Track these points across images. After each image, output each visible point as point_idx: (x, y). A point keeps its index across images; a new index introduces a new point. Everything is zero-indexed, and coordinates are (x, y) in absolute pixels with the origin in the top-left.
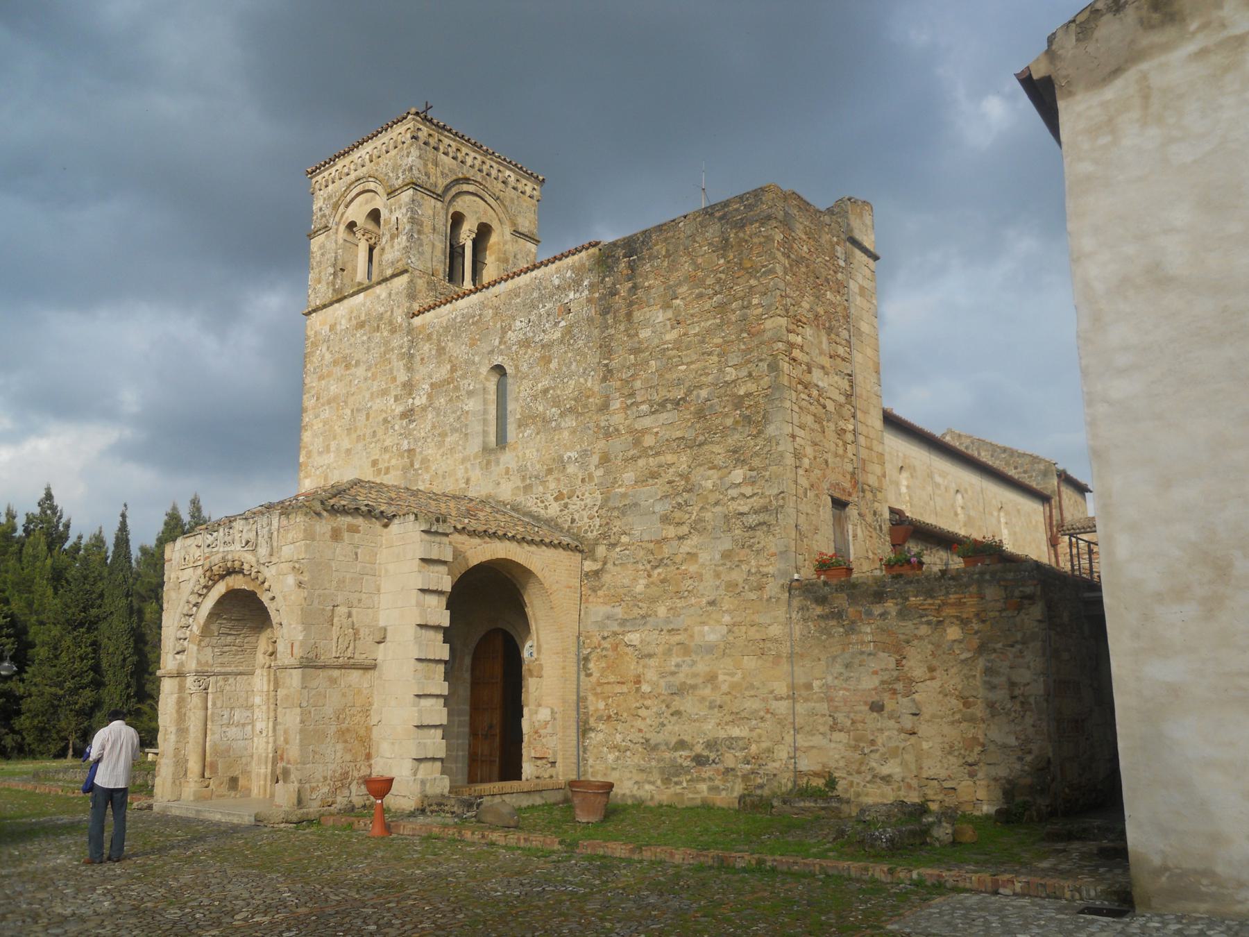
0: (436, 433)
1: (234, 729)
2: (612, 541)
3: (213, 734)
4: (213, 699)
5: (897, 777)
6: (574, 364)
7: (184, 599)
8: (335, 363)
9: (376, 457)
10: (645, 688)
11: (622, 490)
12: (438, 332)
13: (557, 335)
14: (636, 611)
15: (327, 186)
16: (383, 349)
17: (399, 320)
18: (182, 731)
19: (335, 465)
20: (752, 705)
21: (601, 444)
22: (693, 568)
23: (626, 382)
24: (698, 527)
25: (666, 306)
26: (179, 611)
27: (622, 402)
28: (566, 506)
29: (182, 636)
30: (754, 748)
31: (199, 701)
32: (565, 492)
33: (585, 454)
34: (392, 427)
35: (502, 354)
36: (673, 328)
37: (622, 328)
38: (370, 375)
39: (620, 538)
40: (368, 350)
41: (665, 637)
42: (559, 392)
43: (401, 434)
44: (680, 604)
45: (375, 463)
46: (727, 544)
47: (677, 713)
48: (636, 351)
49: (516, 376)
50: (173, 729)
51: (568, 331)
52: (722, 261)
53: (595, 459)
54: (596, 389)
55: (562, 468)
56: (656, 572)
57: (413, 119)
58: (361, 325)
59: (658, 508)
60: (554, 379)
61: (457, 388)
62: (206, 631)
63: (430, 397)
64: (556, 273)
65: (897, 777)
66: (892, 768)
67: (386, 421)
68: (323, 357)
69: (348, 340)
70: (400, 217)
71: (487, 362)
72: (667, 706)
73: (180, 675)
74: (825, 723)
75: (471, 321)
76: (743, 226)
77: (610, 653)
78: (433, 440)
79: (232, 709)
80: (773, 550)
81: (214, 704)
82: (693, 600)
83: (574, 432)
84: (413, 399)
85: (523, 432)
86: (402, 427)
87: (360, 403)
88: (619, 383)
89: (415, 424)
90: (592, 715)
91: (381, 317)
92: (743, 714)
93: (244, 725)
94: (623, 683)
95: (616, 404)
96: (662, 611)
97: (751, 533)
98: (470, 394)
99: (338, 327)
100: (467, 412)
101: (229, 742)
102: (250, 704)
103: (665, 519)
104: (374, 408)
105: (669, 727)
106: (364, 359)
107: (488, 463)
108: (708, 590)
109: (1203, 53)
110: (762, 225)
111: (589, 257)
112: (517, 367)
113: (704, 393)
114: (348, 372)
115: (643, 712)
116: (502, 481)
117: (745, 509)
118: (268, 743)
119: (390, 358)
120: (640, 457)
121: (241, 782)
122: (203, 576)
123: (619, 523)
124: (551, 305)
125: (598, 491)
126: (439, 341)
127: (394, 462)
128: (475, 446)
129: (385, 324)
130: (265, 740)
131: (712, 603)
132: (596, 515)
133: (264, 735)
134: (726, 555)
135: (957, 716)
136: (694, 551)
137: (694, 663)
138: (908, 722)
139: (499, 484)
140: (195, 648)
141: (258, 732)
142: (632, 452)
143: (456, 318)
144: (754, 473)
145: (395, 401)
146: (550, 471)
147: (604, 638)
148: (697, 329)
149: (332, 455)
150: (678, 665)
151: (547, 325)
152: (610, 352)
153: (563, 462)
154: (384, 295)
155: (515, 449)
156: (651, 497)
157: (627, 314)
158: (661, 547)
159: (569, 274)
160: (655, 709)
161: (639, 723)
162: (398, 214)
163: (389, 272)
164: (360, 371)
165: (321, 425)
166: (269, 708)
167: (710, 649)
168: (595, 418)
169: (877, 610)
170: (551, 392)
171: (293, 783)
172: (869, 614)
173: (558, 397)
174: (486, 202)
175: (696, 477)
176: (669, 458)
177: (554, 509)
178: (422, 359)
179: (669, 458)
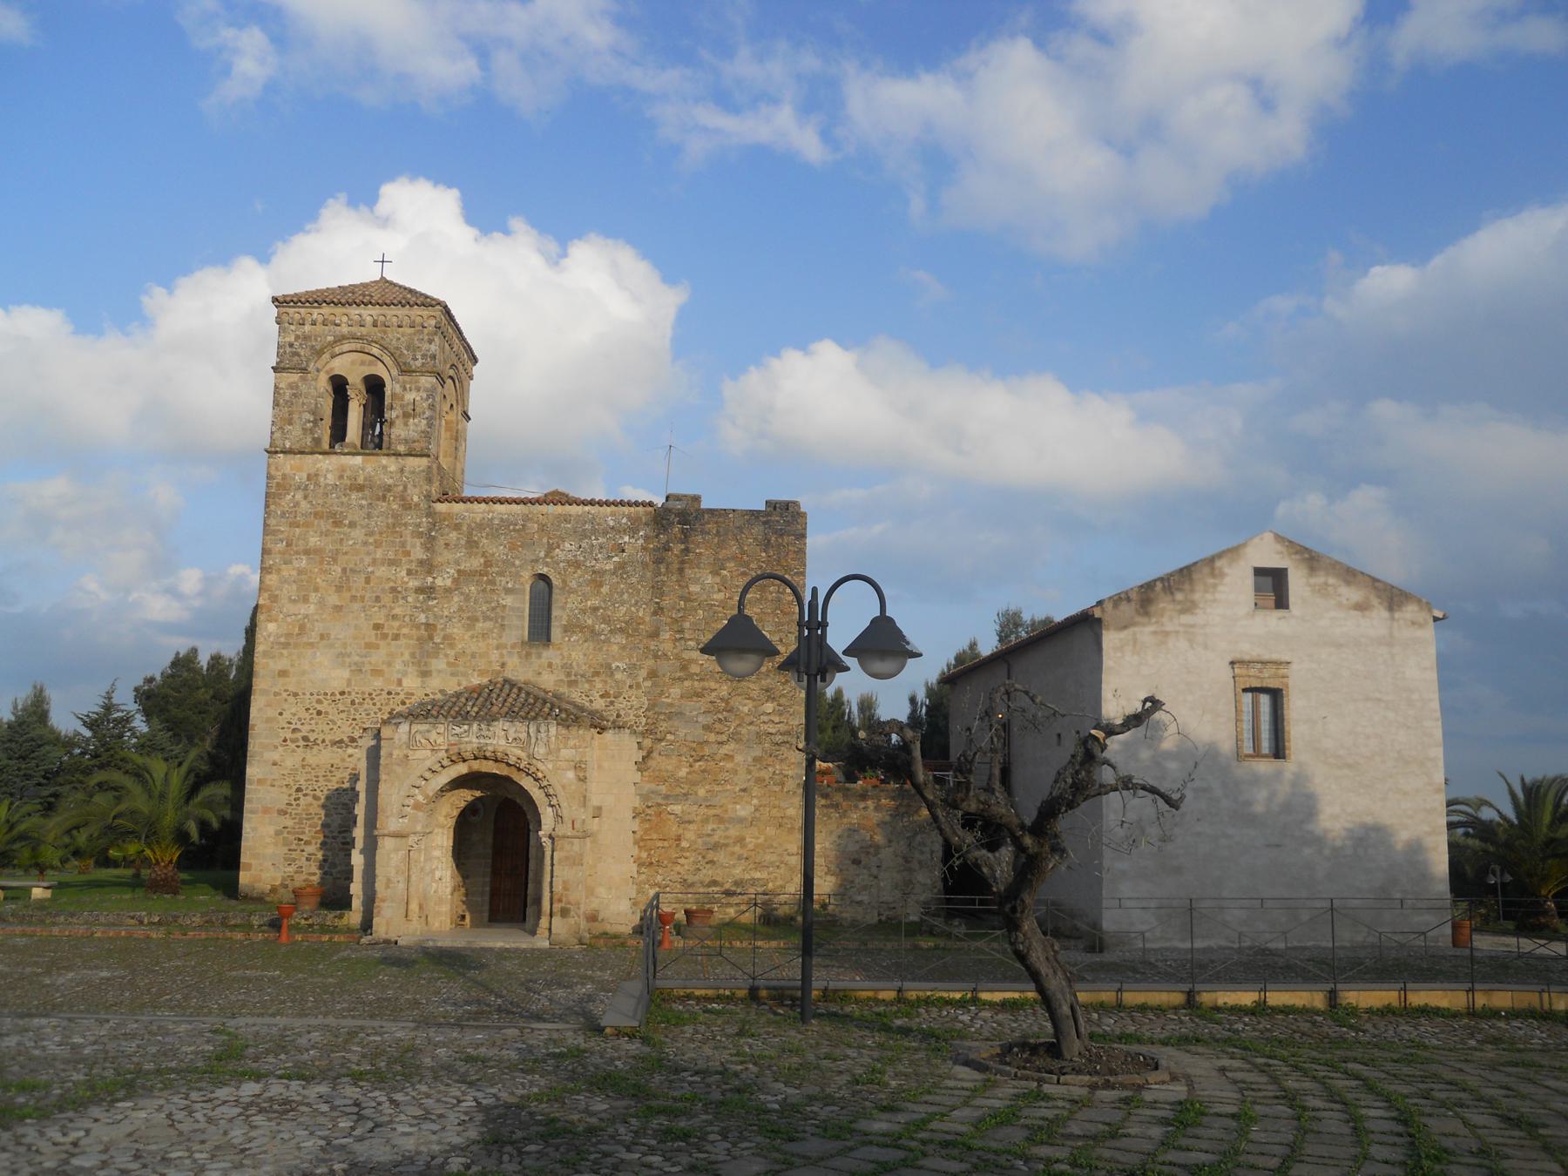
2: (659, 736)
5: (866, 902)
8: (316, 514)
9: (381, 622)
10: (684, 844)
11: (669, 701)
12: (469, 525)
13: (610, 567)
14: (678, 790)
16: (390, 521)
17: (416, 499)
19: (316, 617)
20: (769, 858)
21: (650, 662)
22: (729, 765)
24: (735, 737)
25: (715, 573)
28: (612, 703)
30: (770, 885)
32: (612, 692)
34: (405, 598)
36: (720, 591)
37: (674, 578)
40: (369, 516)
41: (703, 810)
42: (609, 613)
43: (416, 607)
44: (717, 788)
45: (377, 627)
46: (758, 753)
47: (712, 862)
48: (687, 600)
49: (563, 588)
51: (621, 566)
52: (764, 554)
53: (643, 673)
54: (647, 619)
56: (698, 764)
57: (441, 311)
58: (360, 488)
59: (700, 719)
60: (604, 601)
61: (492, 582)
63: (455, 581)
64: (611, 515)
65: (866, 902)
66: (864, 897)
67: (393, 590)
68: (297, 504)
72: (704, 857)
74: (822, 871)
75: (511, 527)
76: (782, 535)
77: (653, 818)
78: (460, 621)
80: (793, 760)
82: (729, 787)
83: (623, 648)
85: (570, 637)
87: (356, 564)
88: (669, 620)
89: (435, 602)
91: (388, 489)
92: (765, 864)
96: (702, 792)
97: (777, 747)
98: (508, 591)
100: (504, 606)
103: (707, 728)
104: (378, 574)
105: (704, 871)
107: (528, 655)
108: (741, 779)
109: (1155, 633)
110: (797, 539)
111: (647, 514)
112: (564, 582)
115: (682, 861)
116: (544, 672)
117: (773, 731)
124: (605, 540)
126: (470, 534)
127: (405, 631)
131: (744, 790)
134: (756, 759)
135: (902, 868)
136: (731, 753)
137: (727, 829)
138: (875, 871)
139: (540, 673)
141: (437, 878)
142: (678, 674)
143: (492, 519)
144: (781, 708)
145: (408, 574)
146: (597, 674)
147: (649, 807)
149: (312, 606)
150: (713, 830)
152: (662, 594)
153: (611, 668)
154: (393, 468)
155: (559, 649)
156: (695, 710)
157: (679, 569)
158: (703, 748)
159: (624, 520)
160: (692, 859)
161: (678, 868)
164: (358, 534)
165: (294, 573)
167: (741, 820)
168: (645, 641)
169: (862, 805)
172: (856, 807)
175: (736, 702)
176: (713, 685)
177: (599, 704)
178: (447, 545)
179: (713, 685)
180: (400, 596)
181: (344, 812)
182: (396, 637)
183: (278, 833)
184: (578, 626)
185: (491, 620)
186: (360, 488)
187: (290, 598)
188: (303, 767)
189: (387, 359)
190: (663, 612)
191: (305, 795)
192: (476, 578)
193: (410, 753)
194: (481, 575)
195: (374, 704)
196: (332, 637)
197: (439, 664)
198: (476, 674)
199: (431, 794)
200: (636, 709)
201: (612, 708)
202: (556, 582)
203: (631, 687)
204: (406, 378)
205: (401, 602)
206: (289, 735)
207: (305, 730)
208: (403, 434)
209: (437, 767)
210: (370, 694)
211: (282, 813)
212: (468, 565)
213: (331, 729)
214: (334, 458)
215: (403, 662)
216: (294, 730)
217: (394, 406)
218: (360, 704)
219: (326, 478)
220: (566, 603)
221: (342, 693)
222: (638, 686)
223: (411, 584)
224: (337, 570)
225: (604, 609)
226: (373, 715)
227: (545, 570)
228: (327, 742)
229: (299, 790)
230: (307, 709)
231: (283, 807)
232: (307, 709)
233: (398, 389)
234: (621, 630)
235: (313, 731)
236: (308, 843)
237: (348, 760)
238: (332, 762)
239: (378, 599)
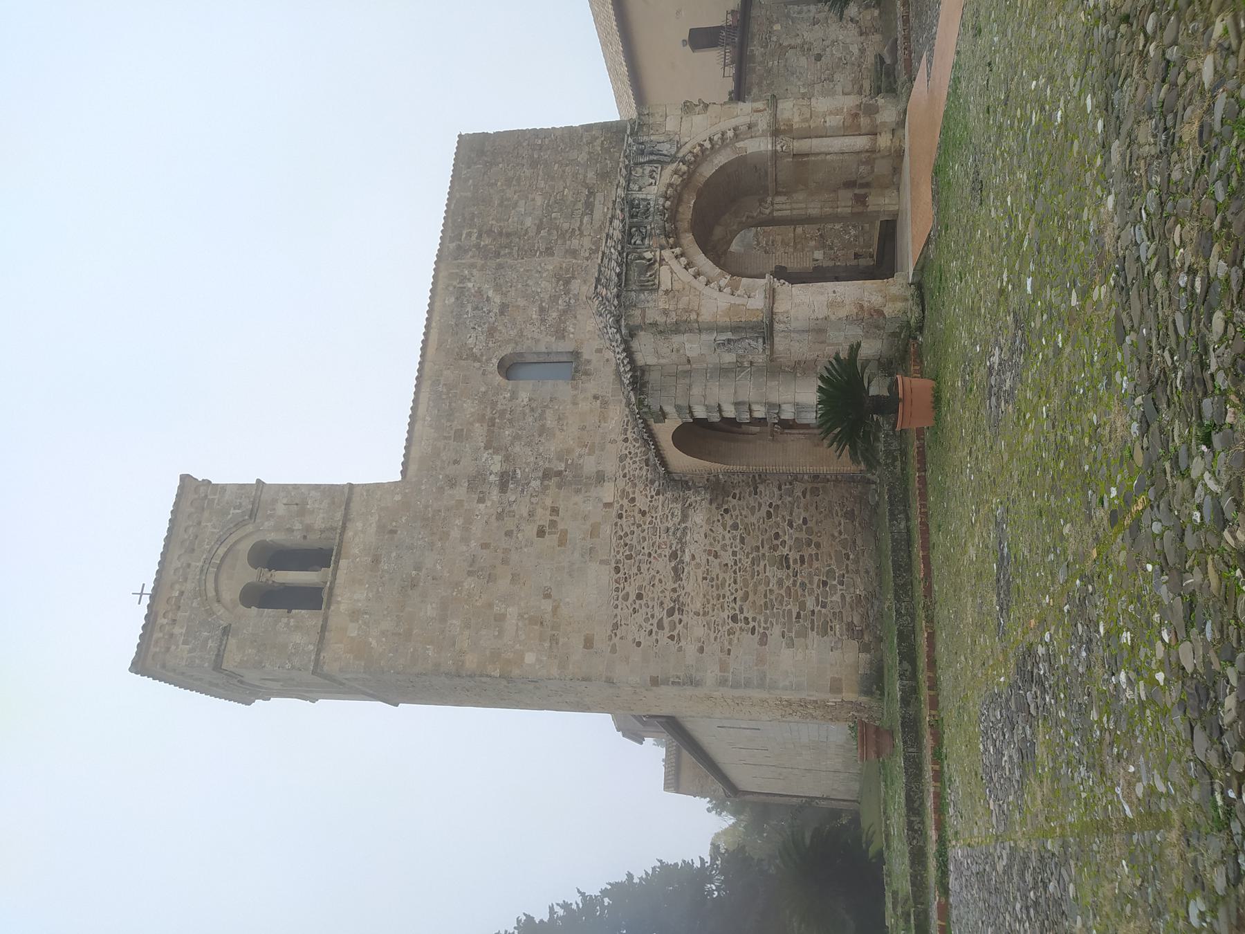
0: (537, 439)
35: (490, 359)
43: (523, 491)
45: (541, 533)
49: (516, 343)
58: (376, 560)
61: (503, 413)
63: (496, 451)
70: (285, 501)
89: (518, 471)
95: (575, 243)
98: (514, 396)
107: (586, 373)
113: (591, 174)
128: (564, 389)
139: (608, 360)
148: (543, 182)
151: (485, 310)
165: (467, 633)
170: (544, 304)
178: (456, 462)
181: (762, 564)
182: (555, 511)
183: (791, 644)
185: (544, 412)
186: (376, 560)
188: (705, 614)
189: (234, 538)
190: (551, 248)
191: (741, 611)
193: (663, 287)
194: (494, 425)
195: (633, 533)
196: (548, 584)
197: (590, 465)
198: (603, 424)
199: (718, 270)
202: (508, 350)
204: (259, 514)
205: (514, 507)
206: (667, 632)
207: (660, 613)
208: (321, 515)
209: (683, 260)
210: (621, 538)
211: (763, 640)
213: (660, 581)
214: (337, 591)
215: (584, 502)
216: (660, 626)
217: (288, 526)
218: (630, 550)
219: (358, 600)
221: (617, 570)
224: (470, 583)
225: (542, 302)
226: (645, 534)
227: (495, 361)
228: (677, 585)
229: (734, 618)
230: (635, 611)
231: (756, 637)
232: (635, 611)
234: (567, 282)
235: (662, 603)
236: (802, 606)
237: (698, 560)
238: (700, 579)
239: (509, 534)
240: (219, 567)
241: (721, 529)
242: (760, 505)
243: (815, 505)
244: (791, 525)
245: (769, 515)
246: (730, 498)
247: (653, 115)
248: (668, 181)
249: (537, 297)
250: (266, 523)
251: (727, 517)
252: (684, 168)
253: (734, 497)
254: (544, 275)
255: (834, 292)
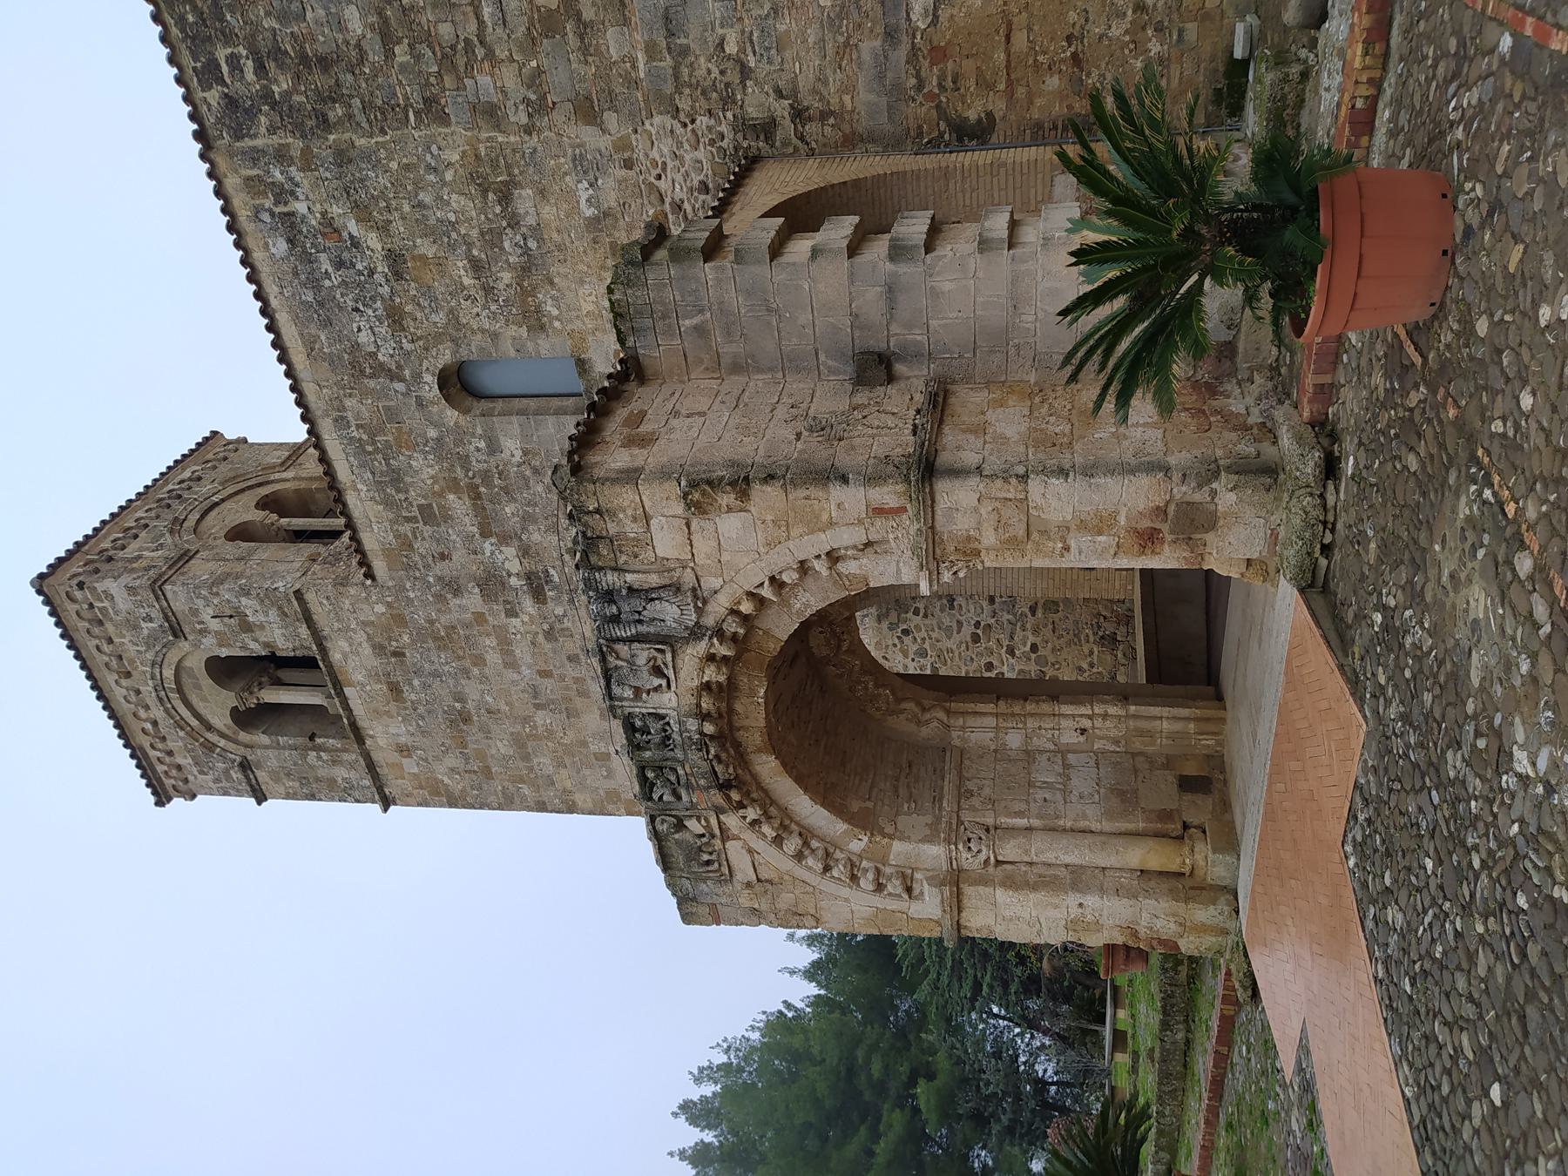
1: (1075, 782)
2: (733, 77)
3: (1085, 817)
4: (1009, 815)
6: (421, 196)
7: (788, 865)
11: (641, 58)
13: (373, 241)
15: (179, 768)
16: (431, 644)
18: (1078, 879)
23: (446, 60)
26: (814, 879)
27: (481, 71)
29: (870, 876)
31: (1013, 842)
33: (583, 165)
34: (560, 619)
35: (419, 375)
38: (476, 671)
39: (729, 57)
40: (436, 674)
42: (475, 233)
50: (1072, 900)
53: (590, 137)
55: (609, 221)
60: (452, 247)
61: (486, 476)
62: (863, 821)
63: (504, 539)
67: (550, 635)
69: (423, 718)
70: (210, 611)
71: (435, 409)
73: (955, 881)
79: (1031, 784)
81: (1020, 814)
84: (509, 575)
85: (552, 318)
86: (558, 599)
89: (552, 572)
90: (1070, 107)
93: (1066, 766)
94: (1010, 25)
98: (493, 448)
99: (403, 740)
100: (525, 453)
101: (1102, 790)
102: (1022, 756)
106: (451, 682)
112: (438, 338)
114: (475, 718)
118: (1105, 716)
119: (446, 628)
120: (579, 14)
121: (1191, 770)
122: (741, 813)
123: (702, 60)
124: (323, 257)
125: (647, 123)
129: (390, 639)
130: (1098, 723)
132: (690, 127)
133: (1087, 723)
140: (897, 846)
141: (1082, 739)
145: (517, 616)
147: (920, 86)
151: (359, 266)
153: (596, 219)
162: (207, 614)
163: (304, 631)
164: (472, 690)
165: (563, 772)
166: (1032, 715)
170: (475, 252)
171: (1214, 493)
173: (482, 234)
174: (223, 500)
178: (443, 557)
180: (558, 626)
184: (524, 302)
187: (606, 777)
192: (489, 506)
193: (739, 877)
194: (478, 496)
199: (842, 826)
200: (680, 145)
201: (686, 206)
203: (628, 164)
204: (186, 629)
212: (467, 520)
220: (483, 331)
222: (623, 145)
223: (531, 610)
224: (542, 718)
225: (470, 245)
227: (430, 379)
233: (209, 641)
234: (505, 198)
240: (179, 690)
241: (900, 657)
242: (960, 623)
243: (1051, 627)
244: (1011, 652)
245: (976, 638)
246: (910, 615)
247: (612, 514)
248: (696, 683)
249: (454, 235)
250: (204, 640)
251: (907, 640)
252: (723, 650)
253: (916, 612)
254: (449, 176)
255: (1081, 905)
